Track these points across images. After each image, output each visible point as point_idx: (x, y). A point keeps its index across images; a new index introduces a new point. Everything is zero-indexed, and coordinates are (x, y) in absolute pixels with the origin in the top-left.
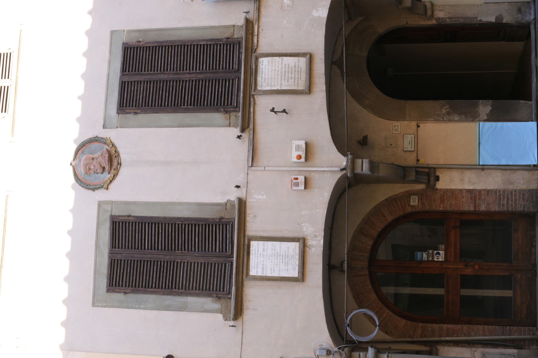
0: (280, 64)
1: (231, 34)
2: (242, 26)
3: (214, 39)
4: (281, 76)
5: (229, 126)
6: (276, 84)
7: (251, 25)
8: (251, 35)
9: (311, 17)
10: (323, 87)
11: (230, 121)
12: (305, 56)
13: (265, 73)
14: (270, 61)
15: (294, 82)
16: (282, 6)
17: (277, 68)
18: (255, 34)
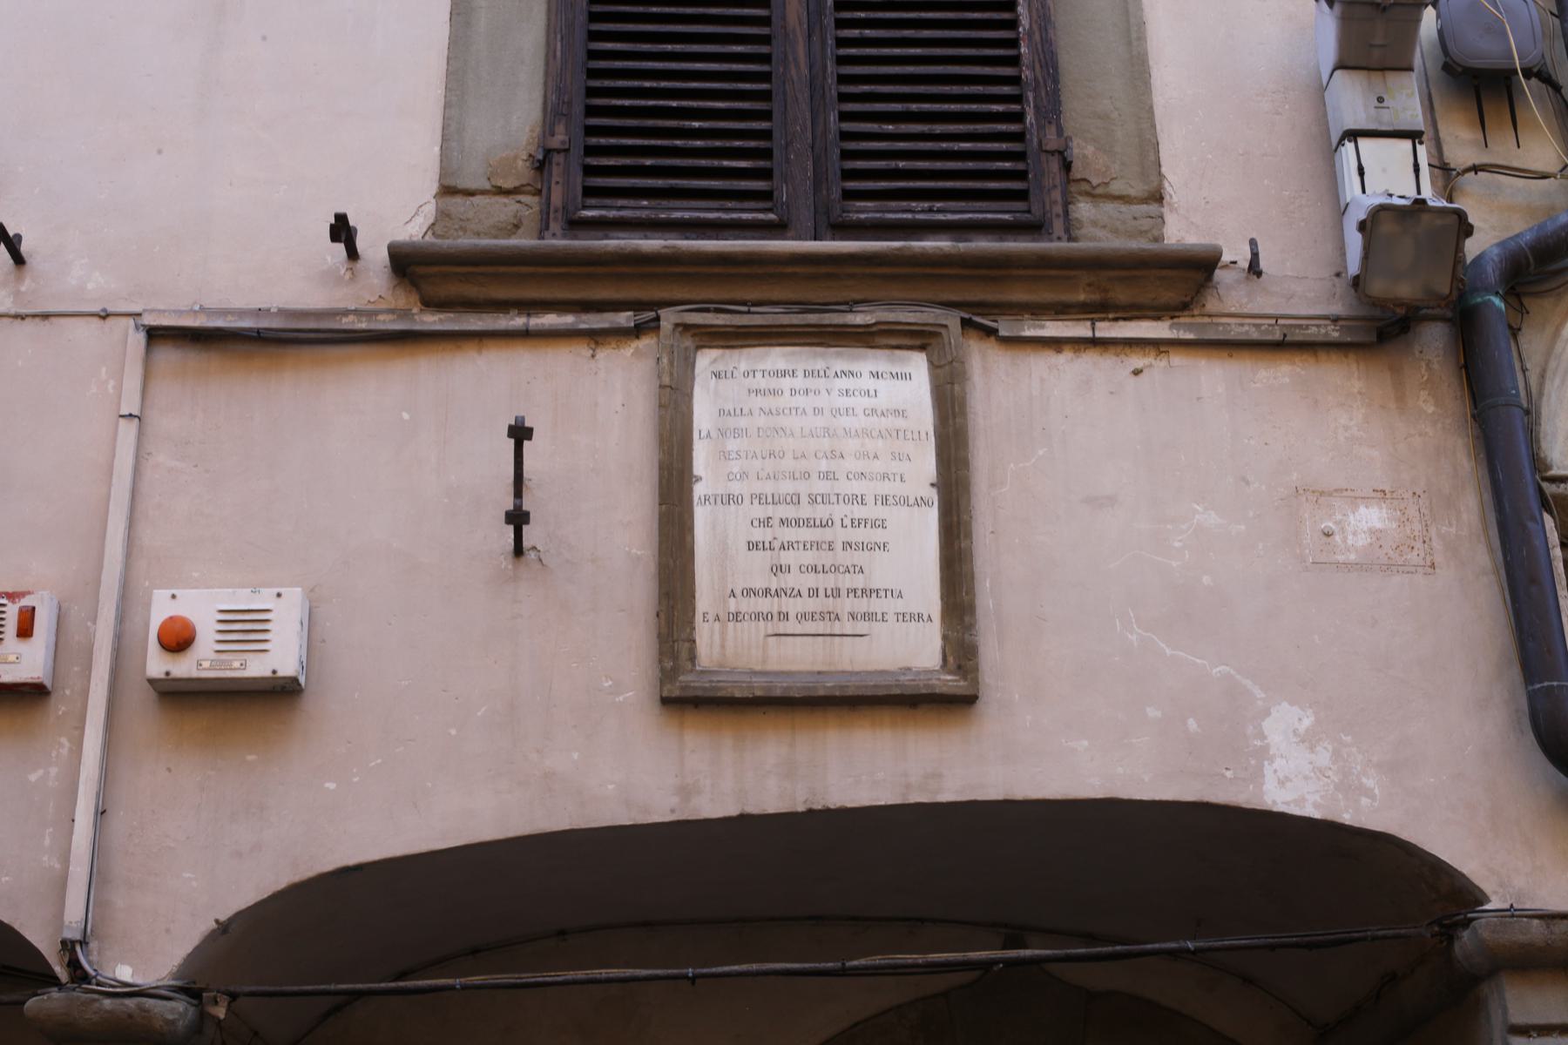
0: (886, 488)
1: (1095, 182)
2: (1158, 239)
3: (1056, 81)
4: (795, 500)
5: (447, 190)
6: (735, 467)
7: (1169, 296)
8: (1096, 297)
9: (1259, 693)
10: (715, 804)
11: (483, 192)
12: (951, 659)
13: (817, 392)
14: (900, 423)
15: (750, 592)
16: (1322, 493)
17: (851, 464)
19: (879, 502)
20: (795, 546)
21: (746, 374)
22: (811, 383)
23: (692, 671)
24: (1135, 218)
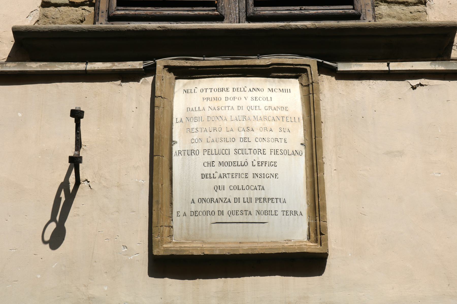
0: (276, 146)
6: (196, 136)
14: (285, 113)
15: (202, 200)
17: (258, 134)
18: (391, 64)
19: (273, 153)
20: (227, 176)
21: (202, 91)
22: (236, 94)
23: (170, 242)
24: (411, 13)
